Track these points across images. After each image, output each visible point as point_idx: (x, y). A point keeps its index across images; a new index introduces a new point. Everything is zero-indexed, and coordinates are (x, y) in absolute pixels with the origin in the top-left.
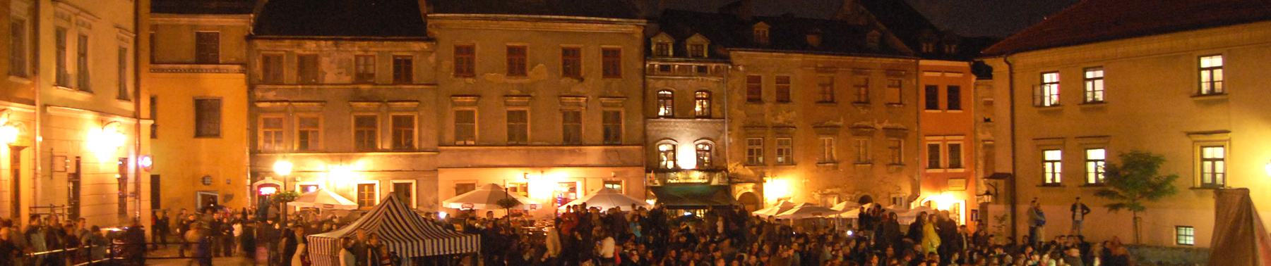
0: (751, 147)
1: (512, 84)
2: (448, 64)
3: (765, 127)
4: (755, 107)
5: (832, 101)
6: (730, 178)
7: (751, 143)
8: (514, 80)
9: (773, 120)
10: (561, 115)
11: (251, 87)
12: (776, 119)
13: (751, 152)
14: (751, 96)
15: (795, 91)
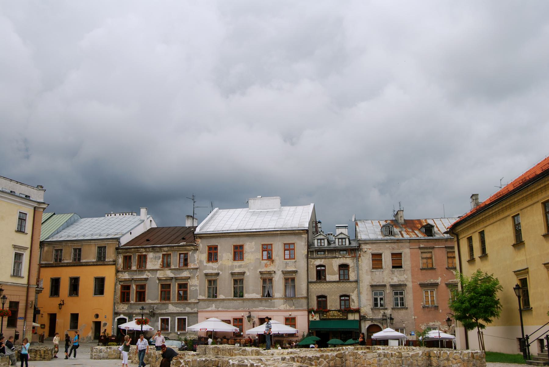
0: (376, 297)
1: (236, 266)
2: (204, 257)
3: (385, 286)
4: (378, 272)
5: (432, 269)
6: (360, 316)
7: (375, 294)
8: (237, 263)
9: (390, 280)
10: (261, 281)
11: (117, 271)
12: (392, 279)
13: (376, 300)
14: (374, 266)
15: (406, 262)
